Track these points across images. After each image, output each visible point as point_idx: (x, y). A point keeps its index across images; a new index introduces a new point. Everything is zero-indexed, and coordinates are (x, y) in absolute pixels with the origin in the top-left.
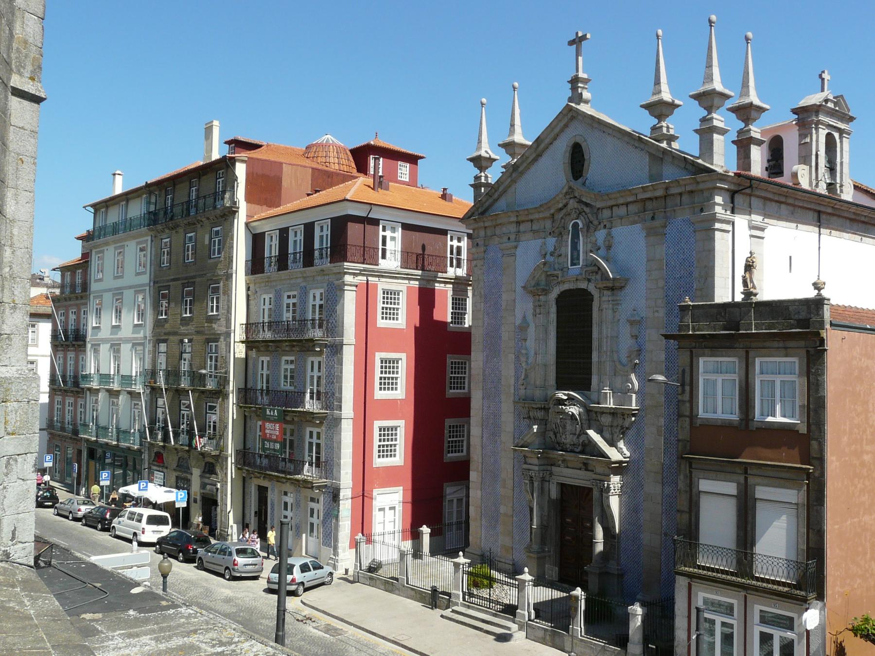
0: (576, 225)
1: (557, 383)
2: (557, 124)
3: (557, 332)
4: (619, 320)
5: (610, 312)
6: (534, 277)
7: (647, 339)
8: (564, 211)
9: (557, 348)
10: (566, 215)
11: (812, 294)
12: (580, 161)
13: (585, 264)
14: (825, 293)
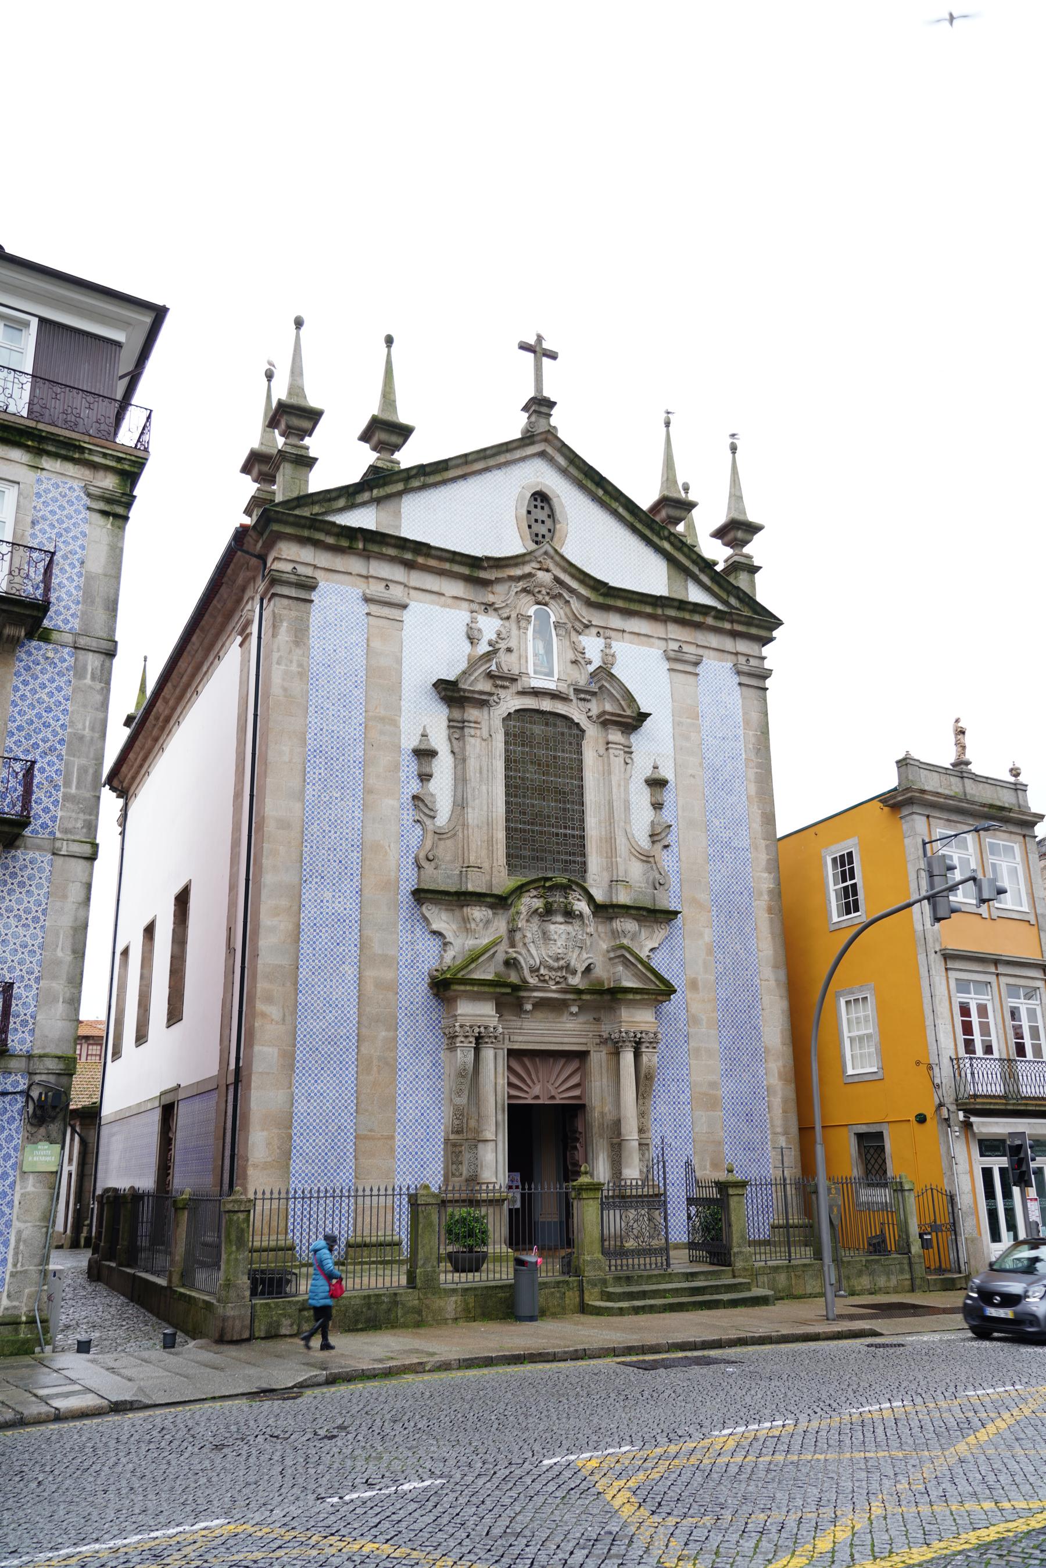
1: (509, 865)
2: (516, 448)
3: (507, 777)
6: (475, 670)
7: (680, 813)
9: (507, 803)
11: (1012, 779)
12: (543, 522)
14: (1022, 779)
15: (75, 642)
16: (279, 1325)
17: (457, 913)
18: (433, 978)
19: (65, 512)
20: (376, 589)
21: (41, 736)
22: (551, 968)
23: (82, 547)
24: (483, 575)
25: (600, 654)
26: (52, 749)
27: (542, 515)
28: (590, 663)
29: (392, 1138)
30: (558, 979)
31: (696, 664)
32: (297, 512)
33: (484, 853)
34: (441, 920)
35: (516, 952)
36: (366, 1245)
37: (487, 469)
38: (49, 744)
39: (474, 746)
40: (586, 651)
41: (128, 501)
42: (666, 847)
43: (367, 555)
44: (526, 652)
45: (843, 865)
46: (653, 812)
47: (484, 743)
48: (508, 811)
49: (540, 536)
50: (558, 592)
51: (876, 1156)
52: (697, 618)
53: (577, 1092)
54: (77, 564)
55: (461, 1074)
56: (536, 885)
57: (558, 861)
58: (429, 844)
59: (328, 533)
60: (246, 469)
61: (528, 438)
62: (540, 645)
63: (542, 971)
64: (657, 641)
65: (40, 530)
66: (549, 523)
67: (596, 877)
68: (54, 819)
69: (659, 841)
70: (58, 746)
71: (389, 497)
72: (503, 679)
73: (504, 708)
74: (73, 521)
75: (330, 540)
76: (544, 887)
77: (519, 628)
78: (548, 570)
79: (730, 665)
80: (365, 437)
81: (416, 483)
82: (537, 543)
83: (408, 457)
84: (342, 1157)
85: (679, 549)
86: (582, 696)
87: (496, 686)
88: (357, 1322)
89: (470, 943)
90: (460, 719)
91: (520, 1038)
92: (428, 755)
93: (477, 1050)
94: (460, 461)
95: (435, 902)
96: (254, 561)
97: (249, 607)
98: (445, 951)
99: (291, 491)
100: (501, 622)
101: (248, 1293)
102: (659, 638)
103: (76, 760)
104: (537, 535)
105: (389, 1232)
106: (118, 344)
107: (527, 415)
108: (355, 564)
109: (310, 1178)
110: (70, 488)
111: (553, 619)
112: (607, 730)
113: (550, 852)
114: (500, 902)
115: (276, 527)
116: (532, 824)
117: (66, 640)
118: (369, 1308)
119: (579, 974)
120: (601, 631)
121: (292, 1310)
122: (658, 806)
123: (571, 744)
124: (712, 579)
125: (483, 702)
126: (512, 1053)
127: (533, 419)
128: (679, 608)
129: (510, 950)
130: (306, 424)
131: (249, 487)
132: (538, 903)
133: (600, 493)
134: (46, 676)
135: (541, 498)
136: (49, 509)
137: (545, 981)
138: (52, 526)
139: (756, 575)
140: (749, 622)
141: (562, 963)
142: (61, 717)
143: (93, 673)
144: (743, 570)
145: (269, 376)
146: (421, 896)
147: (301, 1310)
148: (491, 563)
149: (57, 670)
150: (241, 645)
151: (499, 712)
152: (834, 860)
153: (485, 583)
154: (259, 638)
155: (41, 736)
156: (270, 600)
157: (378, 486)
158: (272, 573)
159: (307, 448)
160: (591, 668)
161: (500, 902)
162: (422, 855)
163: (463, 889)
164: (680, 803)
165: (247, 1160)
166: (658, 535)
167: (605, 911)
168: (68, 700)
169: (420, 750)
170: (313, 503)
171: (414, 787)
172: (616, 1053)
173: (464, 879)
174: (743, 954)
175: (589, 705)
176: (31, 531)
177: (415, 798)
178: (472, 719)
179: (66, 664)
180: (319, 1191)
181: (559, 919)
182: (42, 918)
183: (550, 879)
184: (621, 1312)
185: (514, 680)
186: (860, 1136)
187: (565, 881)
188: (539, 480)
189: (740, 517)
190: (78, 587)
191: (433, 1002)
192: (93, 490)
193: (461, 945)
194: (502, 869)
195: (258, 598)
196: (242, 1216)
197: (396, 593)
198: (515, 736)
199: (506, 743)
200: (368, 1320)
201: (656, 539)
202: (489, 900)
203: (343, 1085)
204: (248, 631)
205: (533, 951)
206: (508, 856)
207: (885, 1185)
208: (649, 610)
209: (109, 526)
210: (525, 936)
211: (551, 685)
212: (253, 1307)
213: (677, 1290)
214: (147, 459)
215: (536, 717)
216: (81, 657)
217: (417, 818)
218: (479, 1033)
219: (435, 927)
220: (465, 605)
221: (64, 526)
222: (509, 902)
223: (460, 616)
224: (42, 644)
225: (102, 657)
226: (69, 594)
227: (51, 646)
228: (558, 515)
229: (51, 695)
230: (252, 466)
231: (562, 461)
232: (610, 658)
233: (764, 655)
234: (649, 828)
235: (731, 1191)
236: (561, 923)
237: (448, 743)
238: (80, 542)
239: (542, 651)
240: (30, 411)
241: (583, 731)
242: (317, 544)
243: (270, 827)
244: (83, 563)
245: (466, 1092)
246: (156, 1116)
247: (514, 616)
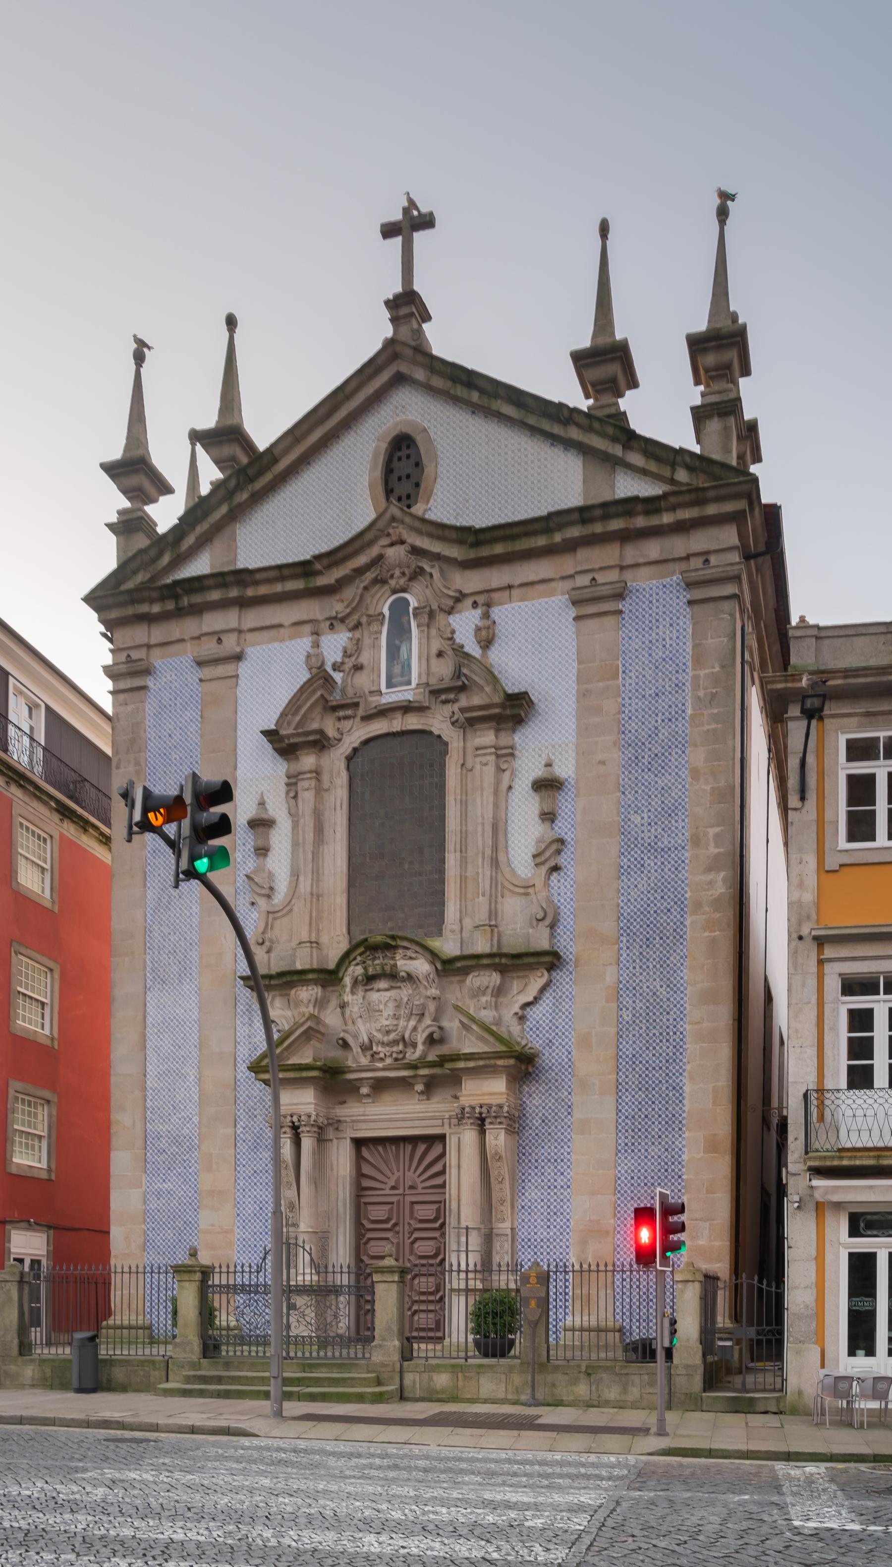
0: (399, 608)
4: (510, 788)
5: (490, 770)
8: (370, 576)
13: (424, 680)
24: (321, 581)
32: (124, 587)
42: (556, 869)
69: (542, 863)
86: (443, 697)
92: (264, 825)
100: (349, 635)
151: (341, 751)
174: (663, 992)
185: (357, 705)
194: (341, 938)
241: (446, 744)
247: (364, 620)
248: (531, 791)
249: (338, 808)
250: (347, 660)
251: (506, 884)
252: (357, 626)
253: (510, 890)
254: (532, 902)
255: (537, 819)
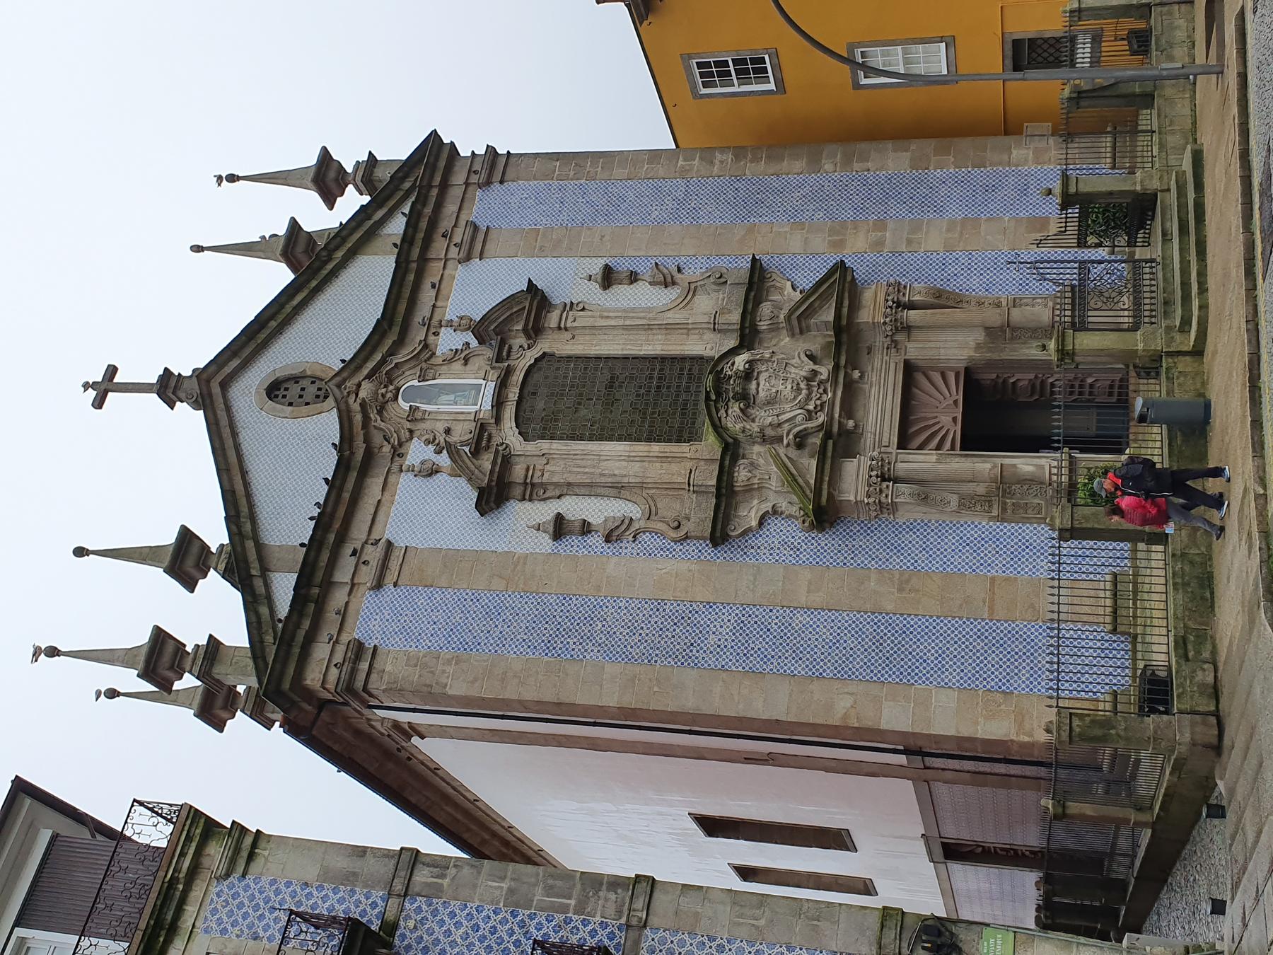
2: (215, 415)
6: (468, 468)
10: (380, 412)
12: (303, 389)
15: (399, 895)
16: (1202, 686)
17: (740, 498)
18: (812, 527)
19: (246, 902)
20: (367, 575)
21: (506, 937)
22: (808, 397)
23: (288, 884)
25: (459, 333)
26: (522, 925)
27: (294, 390)
28: (468, 344)
29: (993, 579)
30: (821, 391)
31: (476, 228)
33: (674, 467)
34: (749, 514)
35: (788, 435)
36: (1115, 612)
37: (237, 448)
38: (516, 928)
39: (554, 473)
40: (454, 348)
41: (238, 829)
42: (679, 270)
43: (328, 585)
44: (451, 413)
45: (711, 75)
46: (640, 283)
47: (552, 462)
48: (628, 438)
49: (319, 393)
50: (387, 377)
51: (1040, 51)
52: (423, 224)
53: (951, 377)
54: (307, 891)
55: (923, 499)
56: (714, 410)
57: (688, 387)
58: (661, 526)
59: (298, 626)
60: (219, 726)
61: (203, 401)
62: (444, 398)
63: (811, 407)
64: (447, 272)
65: (265, 931)
66: (304, 383)
67: (709, 346)
68: (604, 926)
69: (672, 277)
70: (519, 918)
71: (261, 558)
72: (481, 437)
73: (514, 439)
74: (257, 894)
75: (306, 624)
76: (716, 402)
77: (423, 419)
78: (359, 385)
79: (479, 193)
80: (190, 585)
81: (248, 527)
82: (326, 397)
83: (215, 534)
84: (1013, 636)
85: (344, 240)
86: (504, 354)
87: (488, 447)
88: (1203, 598)
89: (774, 484)
90: (522, 488)
91: (886, 435)
92: (561, 524)
93: (896, 480)
94: (225, 477)
95: (727, 520)
96: (324, 715)
97: (377, 724)
98: (782, 513)
99: (246, 666)
101: (1165, 717)
102: (444, 268)
103: (536, 898)
104: (318, 397)
105: (1102, 585)
106: (55, 838)
107: (178, 403)
108: (338, 598)
109: (1036, 672)
110: (218, 895)
111: (415, 383)
112: (544, 328)
113: (677, 396)
114: (731, 451)
115: (286, 685)
116: (645, 414)
117: (396, 906)
118: (1188, 584)
119: (816, 367)
120: (433, 330)
121: (1186, 670)
122: (633, 278)
123: (558, 369)
124: (380, 206)
125: (506, 461)
126: (903, 443)
127: (182, 395)
128: (411, 243)
129: (785, 442)
130: (170, 648)
131: (241, 723)
132: (735, 408)
133: (273, 324)
134: (436, 928)
135: (275, 390)
136: (240, 920)
137: (822, 405)
138: (261, 917)
139: (379, 158)
140: (432, 168)
141: (803, 385)
142: (484, 914)
143: (437, 877)
144: (372, 172)
145: (112, 694)
146: (719, 535)
147: (1187, 659)
148: (346, 446)
149: (430, 917)
150: (423, 737)
151: (518, 447)
152: (705, 85)
153: (369, 455)
154: (414, 710)
155: (506, 937)
156: (371, 695)
157: (248, 568)
158: (339, 690)
159: (197, 646)
160: (474, 343)
161: (731, 451)
162: (673, 534)
163: (714, 490)
164: (631, 253)
165: (1012, 741)
166: (326, 262)
167: (748, 336)
168: (466, 905)
169: (555, 531)
170: (262, 642)
171: (596, 540)
172: (908, 329)
173: (703, 489)
175: (515, 348)
176: (265, 941)
177: (608, 539)
178: (522, 473)
179: (424, 907)
180: (1051, 663)
181: (753, 385)
182: (718, 941)
183: (708, 393)
184: (1204, 307)
185: (482, 427)
186: (1017, 68)
187: (711, 377)
188: (253, 390)
189: (312, 174)
190: (335, 891)
191: (840, 528)
192: (221, 870)
193: (776, 494)
194: (693, 448)
195: (366, 711)
196: (1076, 722)
197: (373, 555)
198: (545, 429)
199: (552, 438)
200: (1202, 586)
201: (330, 266)
202: (727, 462)
203: (930, 631)
204: (406, 727)
205: (788, 416)
206: (679, 441)
207: (1073, 40)
208: (411, 277)
209: (266, 853)
210: (770, 424)
211: (491, 386)
212: (1181, 712)
213: (1181, 249)
214: (191, 807)
215: (526, 405)
216: (417, 889)
217: (631, 538)
218: (877, 477)
219: (754, 523)
220: (392, 479)
221: (262, 903)
222: (731, 440)
223: (405, 483)
224: (398, 933)
225: (419, 866)
226: (341, 901)
227: (402, 923)
228: (296, 371)
229: (458, 925)
230: (215, 716)
231: (235, 363)
232: (464, 322)
233: (469, 154)
234: (657, 288)
235: (1072, 190)
236: (758, 384)
237: (548, 502)
238: (282, 887)
239: (452, 397)
240: (124, 937)
241: (544, 353)
242: (310, 639)
243: (630, 701)
244: (306, 884)
245: (945, 494)
246: (956, 868)
248: (607, 291)
249: (569, 448)
250: (437, 441)
251: (681, 306)
252: (411, 431)
253: (688, 303)
254: (701, 286)
255: (632, 286)
